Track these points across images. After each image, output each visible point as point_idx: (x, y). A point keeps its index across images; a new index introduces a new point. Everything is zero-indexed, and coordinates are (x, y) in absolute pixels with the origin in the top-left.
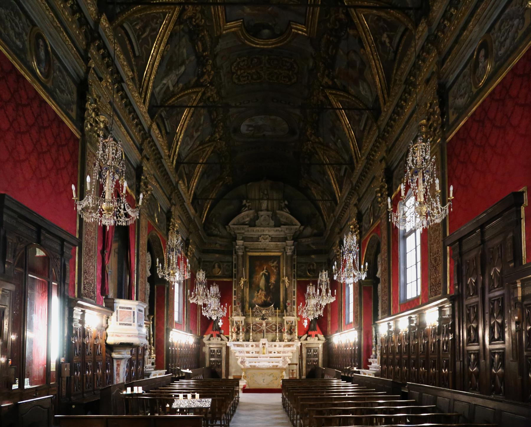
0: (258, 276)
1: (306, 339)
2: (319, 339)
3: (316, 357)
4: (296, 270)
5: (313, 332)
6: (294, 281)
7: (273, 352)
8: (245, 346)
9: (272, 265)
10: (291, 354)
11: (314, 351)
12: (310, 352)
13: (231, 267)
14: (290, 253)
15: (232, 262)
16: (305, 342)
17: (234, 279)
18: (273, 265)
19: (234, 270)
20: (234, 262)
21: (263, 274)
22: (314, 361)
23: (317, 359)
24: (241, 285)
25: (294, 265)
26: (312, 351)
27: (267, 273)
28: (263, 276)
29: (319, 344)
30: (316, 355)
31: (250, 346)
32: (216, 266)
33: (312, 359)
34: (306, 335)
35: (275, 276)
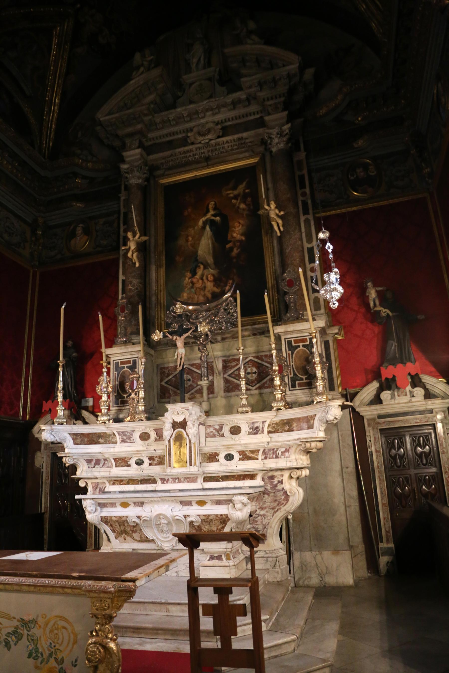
0: (191, 231)
1: (377, 400)
2: (428, 395)
3: (429, 464)
4: (307, 190)
5: (400, 366)
6: (307, 222)
7: (221, 457)
8: (118, 438)
9: (232, 193)
10: (304, 460)
11: (416, 443)
12: (402, 444)
14: (281, 146)
16: (376, 410)
18: (236, 192)
21: (205, 223)
22: (421, 480)
23: (434, 470)
24: (129, 255)
25: (302, 178)
26: (408, 439)
27: (218, 218)
28: (208, 228)
29: (431, 411)
30: (427, 455)
31: (136, 436)
32: (79, 230)
33: (413, 472)
34: (375, 385)
35: (242, 222)
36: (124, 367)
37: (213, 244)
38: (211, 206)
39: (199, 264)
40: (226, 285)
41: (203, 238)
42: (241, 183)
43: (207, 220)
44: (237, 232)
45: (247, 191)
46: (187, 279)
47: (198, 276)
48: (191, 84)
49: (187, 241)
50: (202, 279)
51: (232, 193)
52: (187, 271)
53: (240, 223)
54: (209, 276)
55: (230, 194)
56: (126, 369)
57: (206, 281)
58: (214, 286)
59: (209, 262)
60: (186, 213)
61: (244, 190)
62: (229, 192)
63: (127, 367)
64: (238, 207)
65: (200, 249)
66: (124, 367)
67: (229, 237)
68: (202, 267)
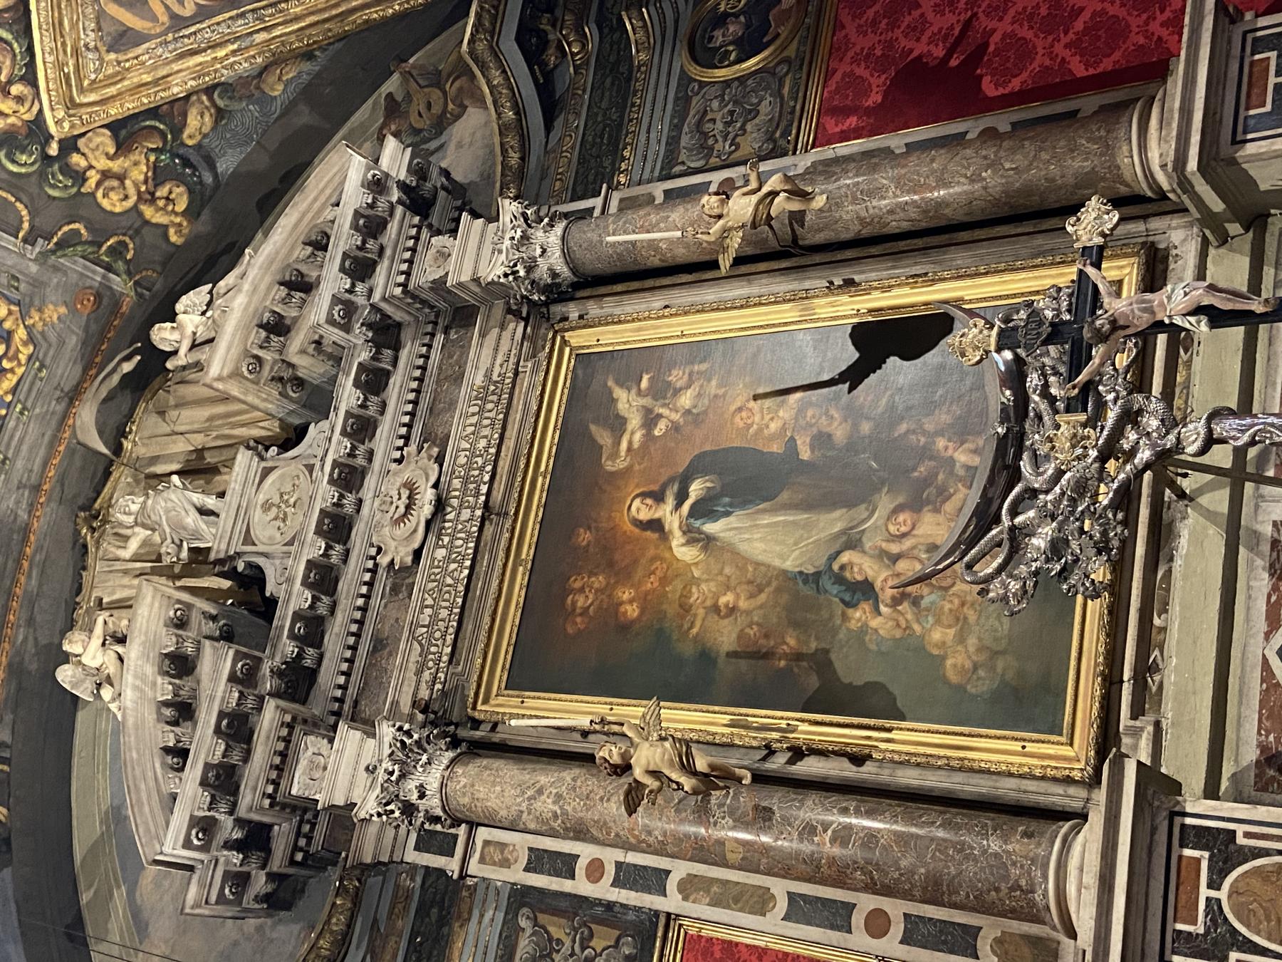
9: (635, 434)
13: (558, 929)
15: (521, 897)
17: (671, 902)
18: (635, 421)
19: (580, 886)
20: (518, 875)
21: (693, 536)
27: (696, 489)
28: (711, 528)
36: (1214, 907)
37: (773, 511)
38: (645, 515)
39: (836, 567)
40: (952, 461)
41: (743, 547)
42: (614, 401)
43: (687, 530)
44: (767, 417)
45: (644, 384)
46: (875, 623)
47: (880, 576)
48: (248, 540)
49: (732, 610)
50: (895, 558)
51: (633, 433)
52: (845, 617)
53: (740, 409)
54: (892, 529)
55: (630, 443)
56: (1223, 894)
57: (907, 543)
58: (937, 510)
59: (838, 527)
60: (632, 611)
61: (639, 393)
62: (624, 445)
63: (1214, 884)
64: (688, 412)
65: (777, 563)
66: (1214, 907)
67: (776, 448)
68: (845, 557)
